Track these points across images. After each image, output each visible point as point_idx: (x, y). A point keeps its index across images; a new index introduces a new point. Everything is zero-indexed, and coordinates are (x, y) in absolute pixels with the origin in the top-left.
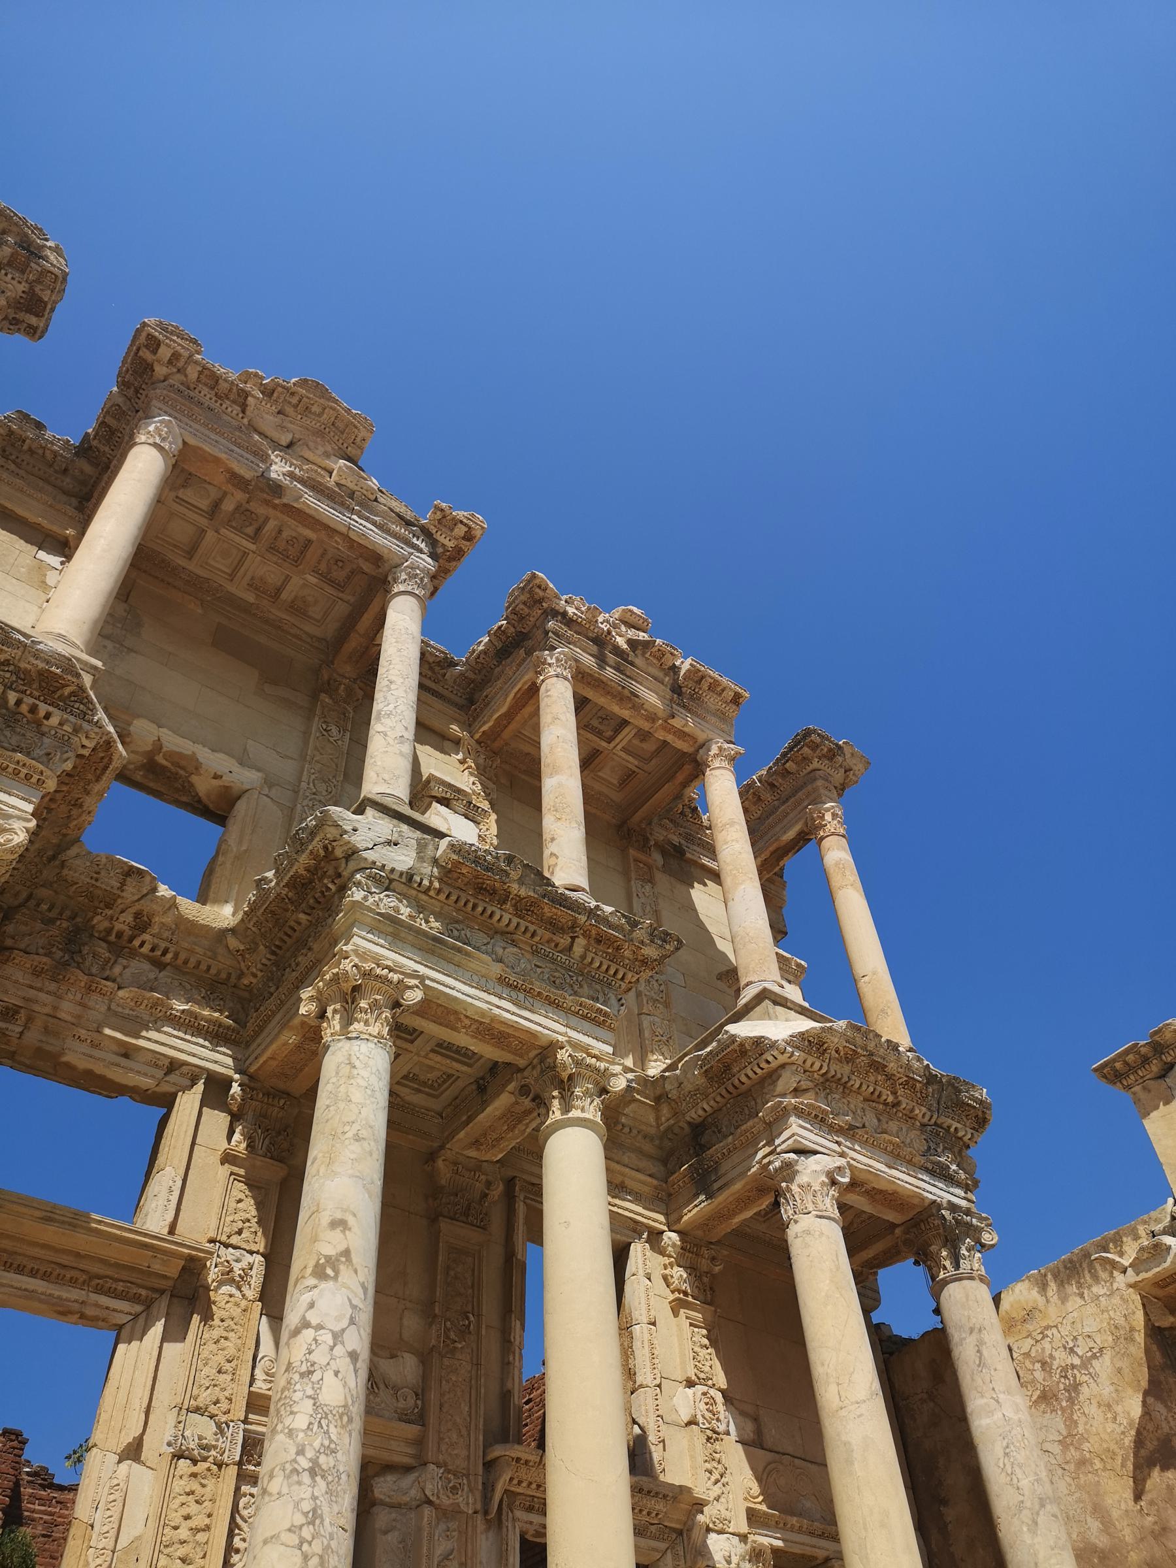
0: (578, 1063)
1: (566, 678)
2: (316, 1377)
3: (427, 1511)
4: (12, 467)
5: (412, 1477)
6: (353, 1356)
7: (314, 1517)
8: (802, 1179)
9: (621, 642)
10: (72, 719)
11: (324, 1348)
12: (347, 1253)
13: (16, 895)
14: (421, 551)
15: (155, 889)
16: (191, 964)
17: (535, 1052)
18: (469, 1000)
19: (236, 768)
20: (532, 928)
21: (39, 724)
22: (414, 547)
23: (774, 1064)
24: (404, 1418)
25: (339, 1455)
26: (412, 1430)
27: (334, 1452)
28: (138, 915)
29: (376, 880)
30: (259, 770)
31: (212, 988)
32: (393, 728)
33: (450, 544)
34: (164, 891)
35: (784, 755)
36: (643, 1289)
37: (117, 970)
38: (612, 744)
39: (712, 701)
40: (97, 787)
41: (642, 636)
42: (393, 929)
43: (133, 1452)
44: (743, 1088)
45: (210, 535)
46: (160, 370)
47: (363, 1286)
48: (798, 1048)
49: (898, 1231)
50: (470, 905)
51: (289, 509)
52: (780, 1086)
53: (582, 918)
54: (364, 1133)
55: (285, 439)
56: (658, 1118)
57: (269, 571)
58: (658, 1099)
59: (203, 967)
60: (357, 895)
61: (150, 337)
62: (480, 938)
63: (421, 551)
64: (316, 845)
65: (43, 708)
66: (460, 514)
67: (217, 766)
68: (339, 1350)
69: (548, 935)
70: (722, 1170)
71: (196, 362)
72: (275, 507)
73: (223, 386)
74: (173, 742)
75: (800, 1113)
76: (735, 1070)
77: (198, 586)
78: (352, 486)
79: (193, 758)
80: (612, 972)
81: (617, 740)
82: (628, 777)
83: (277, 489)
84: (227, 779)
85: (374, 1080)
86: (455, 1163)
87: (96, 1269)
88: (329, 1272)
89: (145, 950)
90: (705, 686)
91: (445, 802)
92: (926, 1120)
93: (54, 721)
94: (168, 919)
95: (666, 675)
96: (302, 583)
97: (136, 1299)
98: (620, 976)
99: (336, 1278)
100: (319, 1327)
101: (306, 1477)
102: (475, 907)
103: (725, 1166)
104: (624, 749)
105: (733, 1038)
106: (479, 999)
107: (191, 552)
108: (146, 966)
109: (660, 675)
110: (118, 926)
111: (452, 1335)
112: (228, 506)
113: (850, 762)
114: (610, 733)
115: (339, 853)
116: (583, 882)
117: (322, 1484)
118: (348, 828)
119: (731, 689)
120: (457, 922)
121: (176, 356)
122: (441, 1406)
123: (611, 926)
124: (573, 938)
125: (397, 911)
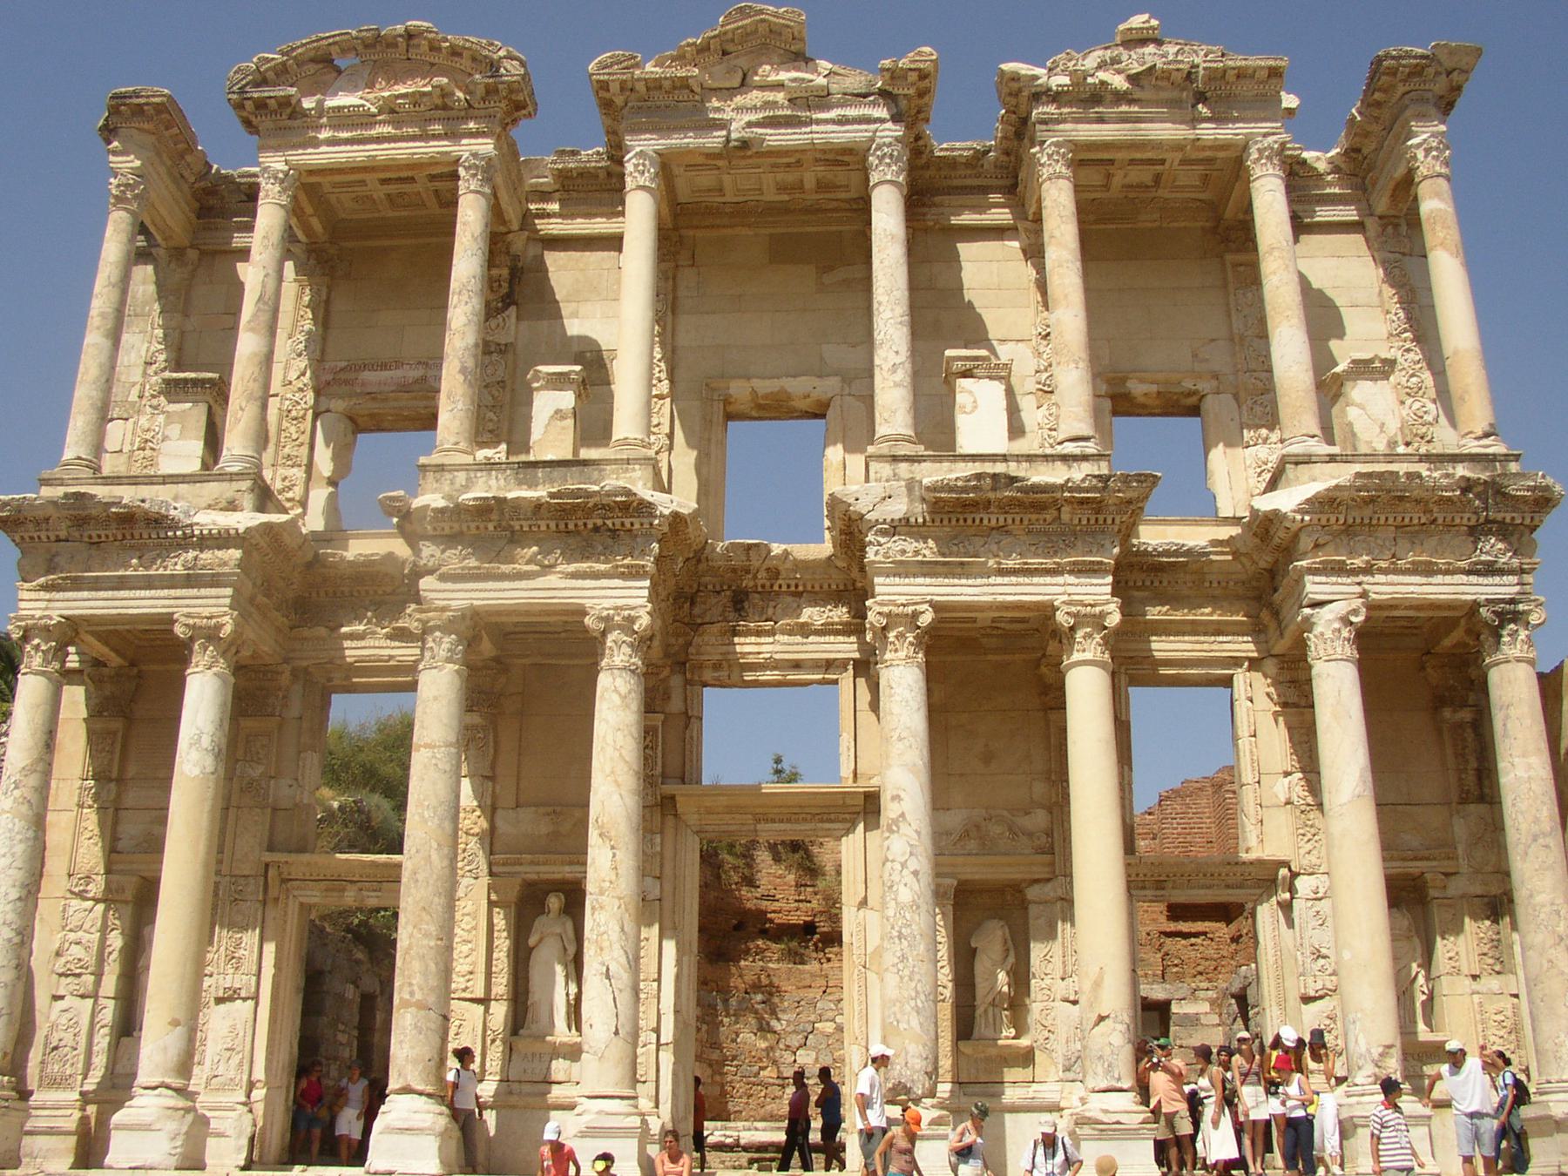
0: (1076, 615)
3: (1059, 904)
4: (574, 194)
5: (1049, 885)
6: (916, 873)
7: (903, 958)
8: (1318, 630)
9: (1119, 82)
10: (645, 520)
12: (903, 815)
14: (882, 121)
15: (769, 551)
16: (817, 588)
24: (1040, 851)
26: (1047, 858)
29: (883, 533)
31: (835, 597)
32: (885, 359)
33: (912, 91)
35: (1368, 85)
37: (770, 611)
39: (1246, 89)
42: (903, 569)
43: (864, 903)
46: (619, 101)
48: (1307, 513)
49: (1463, 622)
53: (1058, 495)
55: (736, 82)
58: (1233, 553)
59: (826, 587)
60: (871, 554)
61: (598, 81)
62: (979, 541)
63: (882, 121)
65: (627, 522)
66: (903, 63)
67: (801, 387)
68: (905, 872)
69: (1034, 517)
73: (667, 84)
74: (765, 386)
77: (742, 213)
79: (783, 391)
82: (1205, 179)
83: (745, 144)
84: (815, 395)
85: (907, 694)
89: (784, 588)
90: (1231, 75)
91: (967, 374)
92: (1473, 523)
93: (637, 526)
94: (788, 565)
95: (1183, 89)
97: (844, 821)
98: (1109, 521)
108: (790, 599)
109: (1175, 94)
110: (760, 583)
116: (1085, 429)
117: (905, 943)
118: (851, 501)
120: (955, 537)
121: (623, 83)
125: (904, 552)
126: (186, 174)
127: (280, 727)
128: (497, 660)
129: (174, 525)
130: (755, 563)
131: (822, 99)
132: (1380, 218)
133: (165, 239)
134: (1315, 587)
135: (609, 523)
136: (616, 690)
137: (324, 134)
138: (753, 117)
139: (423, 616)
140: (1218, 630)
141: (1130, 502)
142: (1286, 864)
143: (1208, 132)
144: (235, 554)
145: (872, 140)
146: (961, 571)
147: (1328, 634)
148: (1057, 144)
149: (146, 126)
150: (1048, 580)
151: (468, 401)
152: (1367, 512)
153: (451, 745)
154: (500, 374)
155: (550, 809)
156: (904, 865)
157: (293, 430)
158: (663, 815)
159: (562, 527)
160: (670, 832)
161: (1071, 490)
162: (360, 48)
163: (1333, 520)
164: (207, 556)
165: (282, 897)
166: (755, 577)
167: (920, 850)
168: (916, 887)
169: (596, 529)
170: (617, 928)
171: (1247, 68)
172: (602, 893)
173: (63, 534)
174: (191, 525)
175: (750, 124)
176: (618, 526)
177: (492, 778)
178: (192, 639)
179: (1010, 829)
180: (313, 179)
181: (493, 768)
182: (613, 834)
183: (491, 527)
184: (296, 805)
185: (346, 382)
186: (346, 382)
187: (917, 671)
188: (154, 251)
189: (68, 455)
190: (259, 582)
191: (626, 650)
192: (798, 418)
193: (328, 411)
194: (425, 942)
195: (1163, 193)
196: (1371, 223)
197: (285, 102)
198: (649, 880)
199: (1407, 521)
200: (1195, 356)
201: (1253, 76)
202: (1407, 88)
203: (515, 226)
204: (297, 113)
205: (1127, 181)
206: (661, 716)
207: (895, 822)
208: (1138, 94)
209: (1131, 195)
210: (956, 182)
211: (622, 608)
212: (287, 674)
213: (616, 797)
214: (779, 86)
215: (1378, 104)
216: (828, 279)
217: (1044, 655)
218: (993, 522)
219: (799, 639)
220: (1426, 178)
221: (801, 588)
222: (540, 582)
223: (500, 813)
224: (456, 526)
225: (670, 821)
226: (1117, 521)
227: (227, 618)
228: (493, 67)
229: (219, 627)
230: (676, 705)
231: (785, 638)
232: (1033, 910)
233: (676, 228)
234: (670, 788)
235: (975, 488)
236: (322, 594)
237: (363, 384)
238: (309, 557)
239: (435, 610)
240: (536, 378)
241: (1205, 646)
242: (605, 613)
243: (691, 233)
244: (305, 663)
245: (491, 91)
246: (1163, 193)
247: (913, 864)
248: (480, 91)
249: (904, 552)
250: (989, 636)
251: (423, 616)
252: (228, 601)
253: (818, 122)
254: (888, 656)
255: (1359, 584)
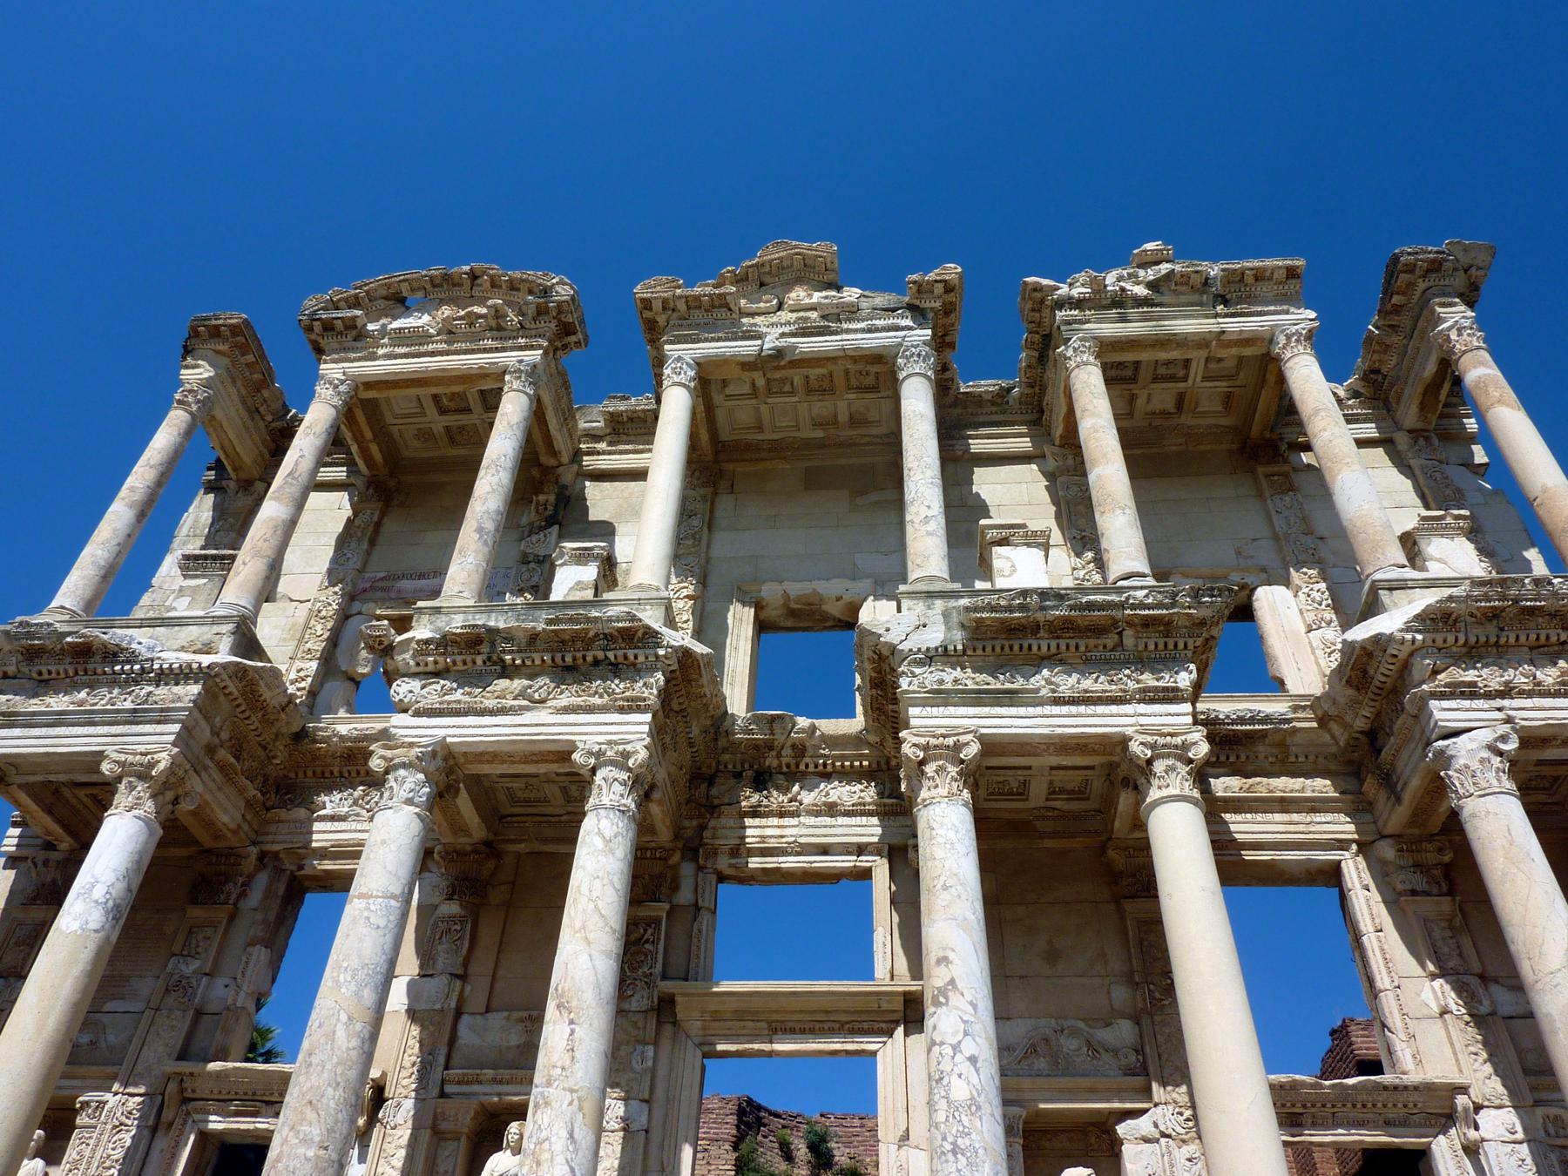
0: (1153, 746)
1: (1086, 364)
2: (945, 1082)
6: (973, 1060)
8: (1460, 762)
9: (1140, 290)
11: (947, 1059)
12: (952, 982)
13: (710, 767)
17: (1118, 749)
18: (1029, 731)
19: (848, 584)
20: (1072, 643)
21: (634, 665)
22: (903, 329)
23: (1403, 655)
25: (973, 1136)
27: (968, 1134)
28: (793, 746)
29: (920, 663)
30: (868, 577)
33: (938, 305)
34: (803, 722)
35: (1385, 292)
36: (1363, 901)
38: (1190, 381)
40: (704, 680)
41: (1165, 268)
42: (941, 697)
43: (906, 1137)
44: (1388, 686)
45: (764, 408)
46: (661, 320)
47: (974, 1006)
48: (1418, 631)
50: (1007, 649)
51: (794, 364)
52: (1416, 674)
54: (950, 882)
56: (1333, 737)
57: (821, 407)
60: (904, 683)
63: (911, 328)
64: (867, 653)
65: (631, 654)
66: (931, 276)
68: (959, 1058)
69: (1092, 642)
70: (1399, 771)
71: (680, 297)
72: (784, 368)
74: (796, 589)
75: (1442, 696)
76: (1372, 672)
77: (778, 449)
78: (835, 311)
80: (1171, 646)
81: (1192, 375)
82: (1228, 399)
83: (779, 353)
84: (847, 598)
86: (1126, 849)
87: (843, 1018)
88: (942, 1000)
89: (811, 768)
90: (1249, 279)
91: (1003, 542)
93: (641, 659)
96: (844, 404)
98: (1181, 646)
99: (947, 1004)
100: (942, 1043)
101: (950, 1157)
102: (1011, 648)
103: (1400, 766)
104: (1205, 379)
105: (1353, 642)
106: (1039, 726)
107: (760, 428)
109: (1196, 297)
110: (784, 760)
111: (1157, 995)
112: (761, 382)
113: (1465, 260)
114: (1181, 374)
115: (885, 652)
117: (962, 1160)
118: (881, 631)
119: (1280, 267)
121: (665, 301)
122: (1160, 1057)
123: (1149, 607)
124: (1120, 634)
125: (941, 682)
126: (262, 409)
127: (232, 918)
128: (488, 844)
129: (133, 658)
130: (780, 738)
131: (852, 312)
132: (1410, 432)
133: (235, 470)
134: (1444, 713)
135: (611, 655)
136: (599, 833)
137: (381, 352)
138: (787, 329)
139: (389, 753)
140: (1314, 806)
141: (1202, 623)
142: (1463, 1090)
143: (1233, 325)
144: (195, 689)
145: (900, 345)
146: (1010, 698)
147: (1475, 765)
148: (1081, 340)
149: (221, 347)
150: (1114, 709)
151: (480, 556)
152: (1491, 629)
153: (393, 897)
154: (536, 579)
155: (525, 1014)
156: (956, 1048)
157: (319, 627)
158: (659, 1022)
159: (558, 660)
160: (666, 1043)
161: (1133, 607)
162: (428, 286)
163: (1451, 639)
164: (162, 692)
165: (179, 1121)
166: (779, 756)
167: (977, 1028)
168: (974, 1079)
169: (596, 662)
170: (564, 1134)
171: (1264, 269)
172: (549, 1084)
173: (11, 670)
174: (152, 660)
175: (783, 335)
176: (620, 659)
177: (463, 978)
178: (119, 779)
179: (1089, 1045)
180: (371, 394)
181: (466, 964)
182: (574, 1003)
183: (479, 660)
184: (228, 1008)
185: (383, 589)
186: (383, 589)
187: (964, 810)
188: (224, 483)
189: (54, 604)
190: (224, 735)
191: (617, 788)
192: (832, 628)
193: (360, 613)
194: (301, 1151)
195: (1186, 419)
196: (1402, 440)
197: (351, 324)
198: (635, 1103)
199: (1543, 638)
200: (1239, 553)
201: (1270, 279)
202: (1426, 285)
203: (565, 459)
204: (361, 335)
205: (1150, 407)
206: (667, 906)
207: (943, 991)
208: (1158, 298)
209: (1156, 423)
210: (981, 419)
211: (616, 743)
212: (254, 857)
213: (584, 958)
214: (813, 308)
215: (1397, 310)
216: (860, 501)
217: (1110, 839)
218: (1044, 649)
219: (827, 820)
220: (1465, 352)
221: (829, 768)
222: (528, 717)
223: (465, 1017)
224: (440, 659)
225: (668, 1030)
226: (1191, 647)
227: (164, 754)
228: (546, 292)
229: (152, 765)
230: (685, 896)
231: (812, 820)
232: (1128, 1150)
233: (716, 461)
234: (667, 986)
235: (1022, 608)
236: (310, 773)
237: (399, 591)
238: (295, 728)
239: (402, 745)
240: (562, 555)
241: (1301, 828)
242: (596, 748)
243: (730, 467)
244: (276, 847)
245: (541, 311)
246: (1186, 419)
247: (969, 1048)
248: (531, 311)
249: (941, 682)
250: (1044, 818)
251: (389, 753)
252: (172, 738)
253: (848, 331)
254: (924, 794)
255: (1499, 709)
